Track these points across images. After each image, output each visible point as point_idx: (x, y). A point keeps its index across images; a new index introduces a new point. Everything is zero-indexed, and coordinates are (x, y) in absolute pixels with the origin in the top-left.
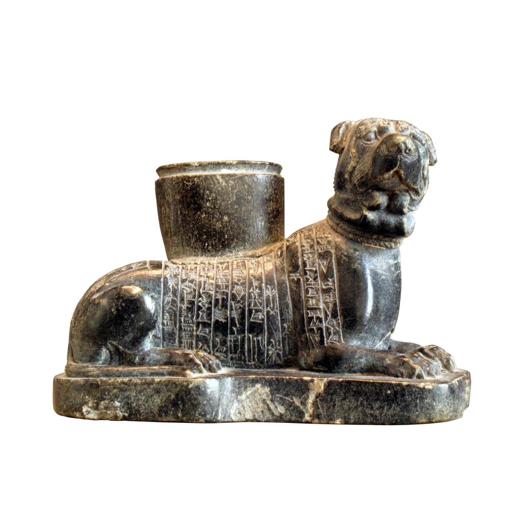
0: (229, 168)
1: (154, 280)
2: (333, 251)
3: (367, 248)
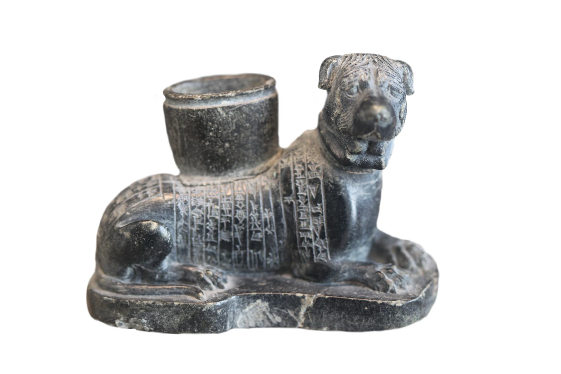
0: (229, 100)
1: (167, 210)
2: (321, 178)
3: (351, 175)
